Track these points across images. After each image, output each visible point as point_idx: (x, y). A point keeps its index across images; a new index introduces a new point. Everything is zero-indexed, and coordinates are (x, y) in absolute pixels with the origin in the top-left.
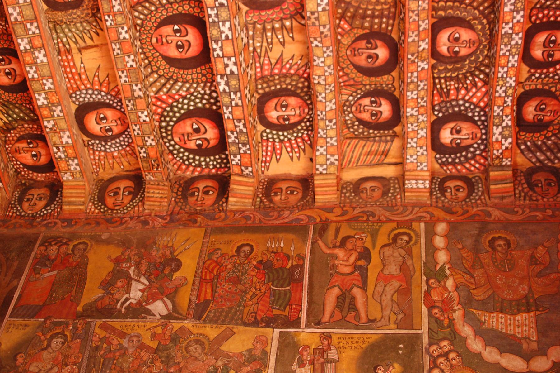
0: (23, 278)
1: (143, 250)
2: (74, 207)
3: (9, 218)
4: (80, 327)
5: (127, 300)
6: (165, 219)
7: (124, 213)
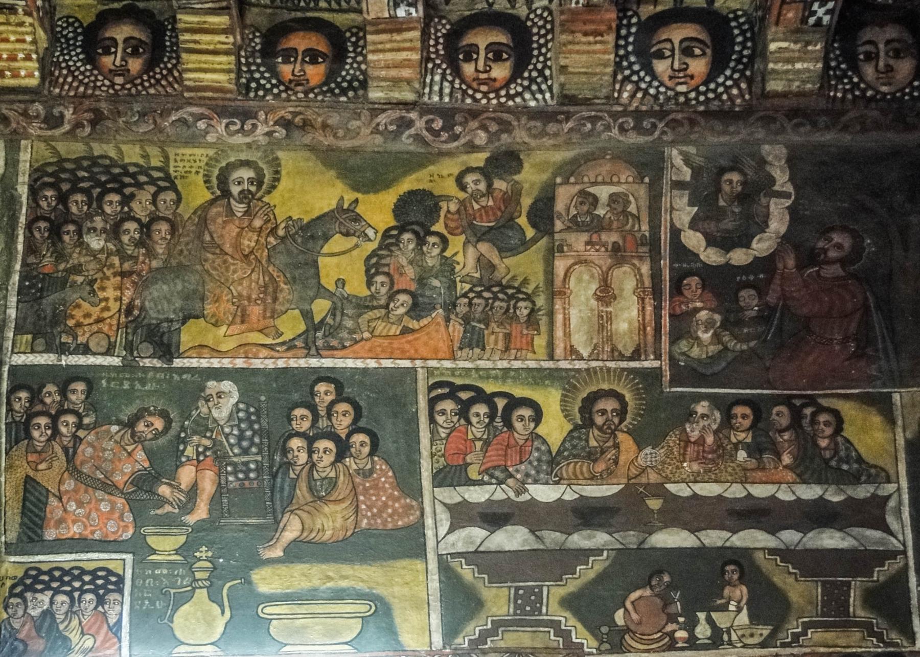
3: (838, 106)
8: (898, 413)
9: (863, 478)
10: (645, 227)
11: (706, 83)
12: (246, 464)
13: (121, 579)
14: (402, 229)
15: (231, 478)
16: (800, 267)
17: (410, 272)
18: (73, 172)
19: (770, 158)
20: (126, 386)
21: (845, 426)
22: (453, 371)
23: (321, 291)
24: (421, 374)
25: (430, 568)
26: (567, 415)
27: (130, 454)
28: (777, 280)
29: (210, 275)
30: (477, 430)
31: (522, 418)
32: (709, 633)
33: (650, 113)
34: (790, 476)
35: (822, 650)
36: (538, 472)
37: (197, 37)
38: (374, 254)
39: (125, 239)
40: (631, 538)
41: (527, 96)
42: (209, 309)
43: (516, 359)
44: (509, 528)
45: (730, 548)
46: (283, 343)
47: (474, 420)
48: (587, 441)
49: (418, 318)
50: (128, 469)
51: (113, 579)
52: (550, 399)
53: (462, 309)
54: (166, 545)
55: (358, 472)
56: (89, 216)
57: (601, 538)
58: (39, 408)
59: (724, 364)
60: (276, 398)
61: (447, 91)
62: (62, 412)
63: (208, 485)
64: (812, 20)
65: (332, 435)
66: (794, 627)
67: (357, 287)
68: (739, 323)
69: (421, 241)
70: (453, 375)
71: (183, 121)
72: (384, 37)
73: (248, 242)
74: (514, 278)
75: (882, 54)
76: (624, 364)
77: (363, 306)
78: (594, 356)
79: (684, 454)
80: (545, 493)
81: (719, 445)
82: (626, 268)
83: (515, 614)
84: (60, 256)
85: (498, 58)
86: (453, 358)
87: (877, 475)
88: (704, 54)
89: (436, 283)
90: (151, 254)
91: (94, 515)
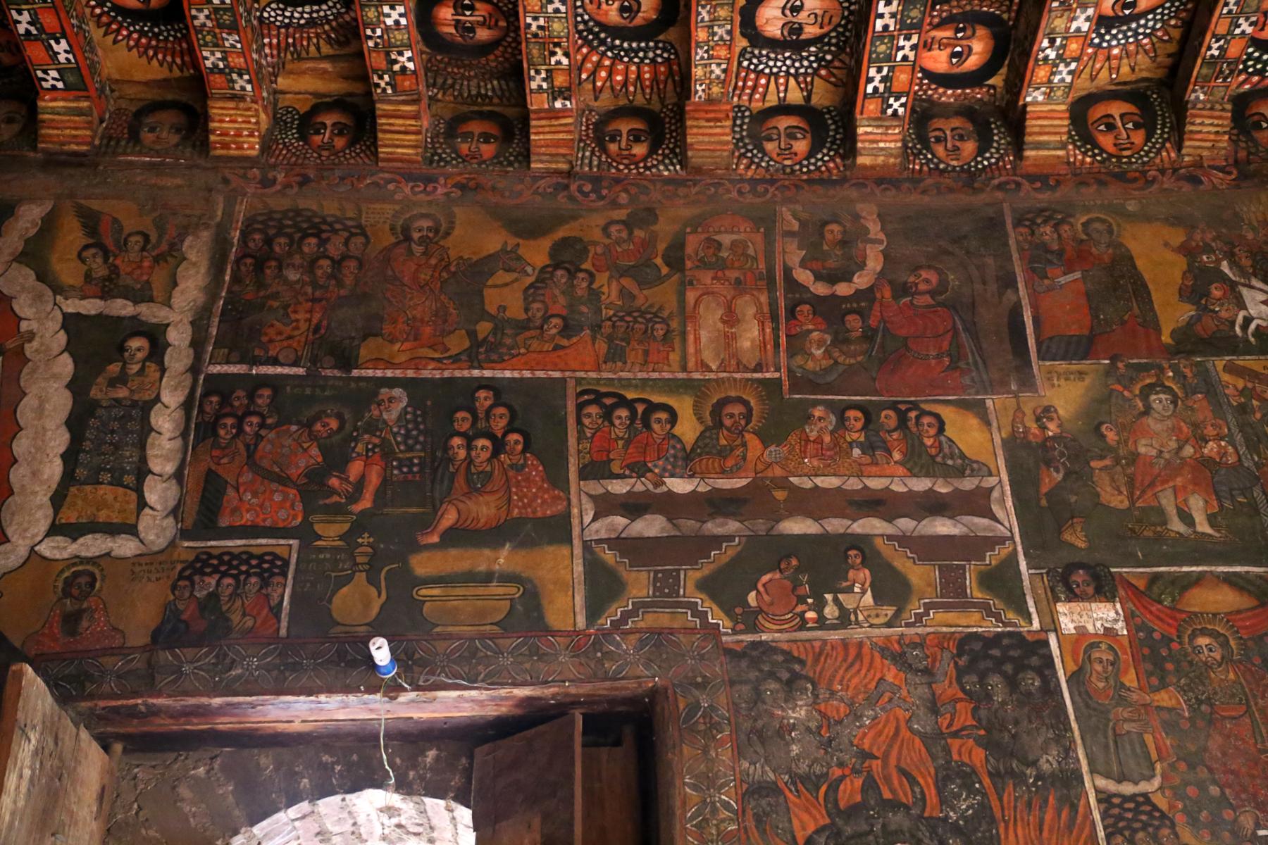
0: (1021, 286)
1: (1224, 230)
2: (1046, 153)
3: (916, 176)
4: (1187, 372)
5: (1248, 320)
6: (1229, 173)
7: (1144, 163)
8: (992, 417)
9: (968, 472)
10: (762, 266)
11: (807, 158)
12: (410, 459)
13: (286, 563)
14: (557, 266)
15: (396, 472)
16: (896, 297)
17: (562, 300)
18: (280, 221)
19: (864, 214)
20: (308, 391)
21: (946, 427)
22: (598, 380)
23: (484, 315)
24: (571, 384)
25: (575, 552)
26: (700, 419)
27: (305, 450)
28: (877, 307)
29: (390, 301)
30: (619, 430)
31: (659, 421)
32: (837, 614)
33: (763, 181)
34: (901, 470)
35: (944, 629)
36: (674, 467)
37: (391, 121)
38: (531, 286)
39: (319, 273)
40: (761, 526)
41: (661, 167)
42: (387, 328)
43: (654, 371)
44: (647, 516)
45: (852, 535)
46: (450, 357)
47: (617, 422)
48: (718, 439)
49: (569, 337)
50: (302, 464)
51: (279, 563)
52: (684, 406)
53: (607, 328)
54: (330, 532)
55: (511, 466)
56: (290, 254)
57: (733, 526)
58: (228, 410)
59: (835, 376)
60: (440, 404)
61: (595, 163)
62: (249, 413)
63: (374, 479)
64: (890, 111)
65: (490, 436)
66: (915, 607)
67: (515, 310)
68: (847, 341)
69: (572, 274)
70: (598, 384)
71: (375, 184)
72: (543, 122)
73: (424, 276)
74: (651, 306)
75: (949, 138)
76: (749, 375)
77: (523, 326)
78: (723, 367)
79: (805, 452)
80: (680, 486)
81: (836, 444)
82: (747, 297)
83: (654, 596)
84: (260, 285)
85: (637, 140)
86: (599, 370)
87: (979, 469)
88: (805, 137)
89: (584, 309)
90: (340, 284)
91: (267, 504)
